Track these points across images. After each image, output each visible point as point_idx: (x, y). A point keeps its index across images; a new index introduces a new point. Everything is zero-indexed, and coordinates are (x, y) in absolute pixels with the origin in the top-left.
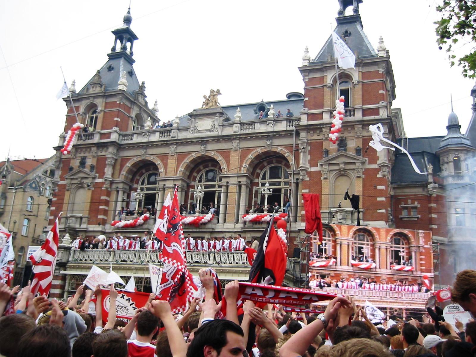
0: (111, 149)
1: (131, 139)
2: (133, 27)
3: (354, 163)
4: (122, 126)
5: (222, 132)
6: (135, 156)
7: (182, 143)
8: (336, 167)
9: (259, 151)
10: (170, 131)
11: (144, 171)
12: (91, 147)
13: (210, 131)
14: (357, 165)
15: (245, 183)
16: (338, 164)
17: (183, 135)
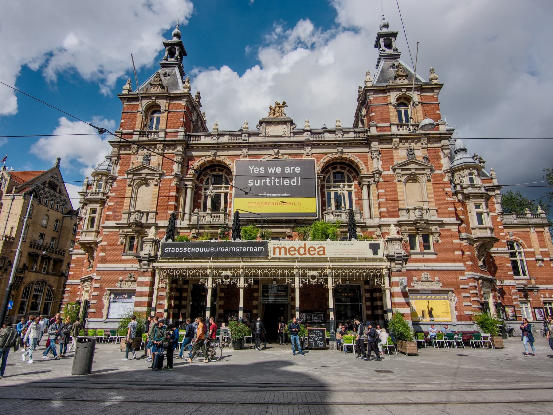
1: (198, 140)
3: (424, 169)
6: (201, 158)
7: (255, 146)
8: (409, 172)
9: (331, 156)
13: (281, 136)
14: (427, 170)
16: (409, 169)
17: (252, 139)
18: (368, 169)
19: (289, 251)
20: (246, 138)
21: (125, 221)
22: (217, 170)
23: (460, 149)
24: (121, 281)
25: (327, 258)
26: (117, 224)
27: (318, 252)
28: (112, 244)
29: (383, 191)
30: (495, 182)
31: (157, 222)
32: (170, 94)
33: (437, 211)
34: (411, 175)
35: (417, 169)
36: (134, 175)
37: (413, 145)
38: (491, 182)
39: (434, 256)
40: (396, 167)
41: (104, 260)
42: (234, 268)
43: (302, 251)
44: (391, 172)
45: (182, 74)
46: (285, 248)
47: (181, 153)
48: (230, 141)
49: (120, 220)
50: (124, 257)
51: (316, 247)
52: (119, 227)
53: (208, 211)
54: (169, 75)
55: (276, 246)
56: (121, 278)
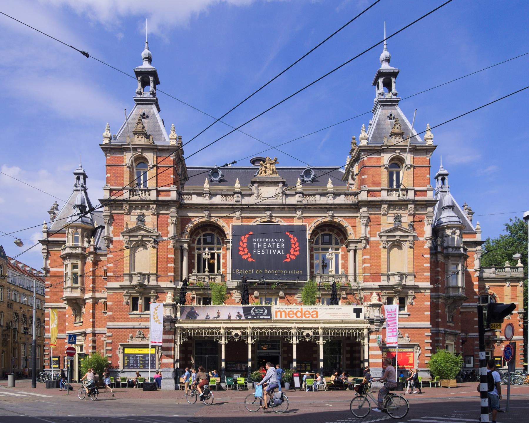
5: (285, 199)
12: (149, 204)
16: (394, 236)
18: (355, 233)
19: (289, 314)
20: (239, 199)
21: (127, 283)
22: (209, 230)
23: (447, 206)
24: (132, 337)
25: (319, 320)
26: (120, 285)
27: (312, 315)
28: (118, 304)
29: (368, 257)
30: (479, 238)
31: (159, 283)
32: (156, 146)
33: (415, 276)
34: (394, 241)
36: (130, 236)
38: (475, 237)
39: (407, 316)
40: (383, 234)
41: (112, 319)
42: (243, 328)
43: (299, 314)
44: (377, 238)
45: (159, 110)
46: (285, 312)
47: (176, 215)
48: (223, 202)
49: (122, 281)
50: (131, 316)
51: (311, 311)
52: (122, 288)
53: (207, 273)
54: (148, 117)
55: (278, 310)
56: (130, 335)
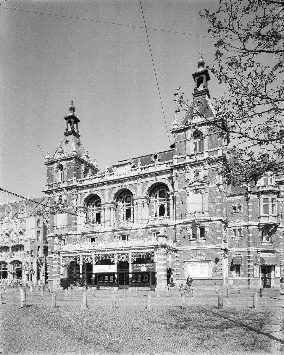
0: (74, 190)
2: (77, 114)
3: (204, 185)
4: (78, 176)
8: (194, 188)
10: (104, 176)
11: (93, 200)
15: (146, 202)
16: (195, 186)
35: (199, 186)
37: (198, 168)
